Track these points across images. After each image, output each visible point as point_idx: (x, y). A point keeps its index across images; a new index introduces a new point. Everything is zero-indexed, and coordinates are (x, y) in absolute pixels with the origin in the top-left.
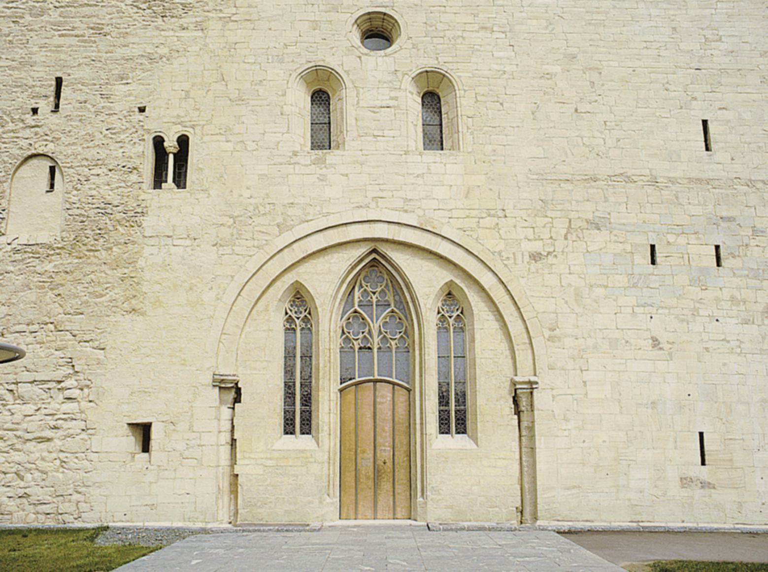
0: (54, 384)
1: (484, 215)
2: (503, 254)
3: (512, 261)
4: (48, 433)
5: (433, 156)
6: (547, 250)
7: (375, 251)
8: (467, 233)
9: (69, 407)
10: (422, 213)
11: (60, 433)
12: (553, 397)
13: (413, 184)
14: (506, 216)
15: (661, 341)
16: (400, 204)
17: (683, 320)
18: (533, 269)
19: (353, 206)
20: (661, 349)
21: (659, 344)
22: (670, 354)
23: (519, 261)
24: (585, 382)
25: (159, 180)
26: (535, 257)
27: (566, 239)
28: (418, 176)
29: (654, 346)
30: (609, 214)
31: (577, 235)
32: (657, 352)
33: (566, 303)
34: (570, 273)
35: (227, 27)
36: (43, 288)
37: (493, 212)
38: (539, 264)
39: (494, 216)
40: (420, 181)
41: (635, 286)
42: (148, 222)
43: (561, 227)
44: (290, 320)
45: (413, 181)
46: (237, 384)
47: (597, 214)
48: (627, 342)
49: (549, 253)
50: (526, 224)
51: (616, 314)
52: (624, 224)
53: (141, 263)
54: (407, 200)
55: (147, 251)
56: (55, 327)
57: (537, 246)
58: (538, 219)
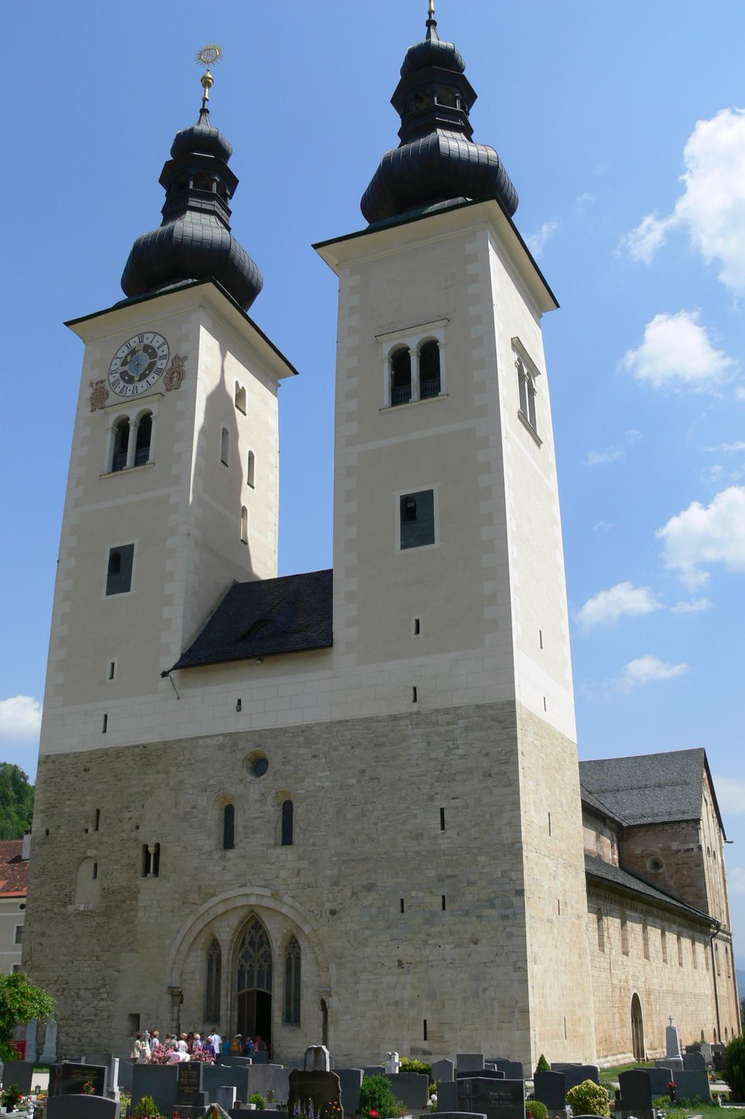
0: (95, 991)
1: (306, 887)
2: (316, 912)
3: (319, 916)
4: (93, 1018)
5: (280, 851)
6: (340, 907)
7: (253, 911)
8: (297, 899)
9: (103, 1004)
10: (273, 888)
11: (98, 1018)
12: (339, 1000)
13: (270, 869)
14: (317, 887)
15: (403, 962)
16: (262, 883)
17: (417, 948)
18: (331, 921)
19: (239, 885)
20: (403, 968)
21: (402, 964)
22: (409, 972)
23: (324, 916)
24: (357, 991)
25: (146, 871)
26: (333, 913)
27: (350, 899)
28: (272, 864)
29: (399, 966)
30: (376, 880)
31: (357, 897)
32: (399, 970)
33: (349, 941)
34: (352, 922)
35: (180, 770)
36: (91, 936)
37: (311, 885)
38: (334, 917)
39: (312, 887)
40: (273, 867)
41: (388, 928)
42: (140, 896)
43: (348, 892)
44: (211, 956)
45: (270, 867)
46: (181, 993)
47: (370, 881)
48: (383, 964)
49: (341, 909)
50: (327, 892)
51: (377, 946)
52: (385, 887)
53: (137, 922)
54: (266, 880)
55: (141, 914)
56: (97, 958)
57: (334, 906)
58: (335, 887)
